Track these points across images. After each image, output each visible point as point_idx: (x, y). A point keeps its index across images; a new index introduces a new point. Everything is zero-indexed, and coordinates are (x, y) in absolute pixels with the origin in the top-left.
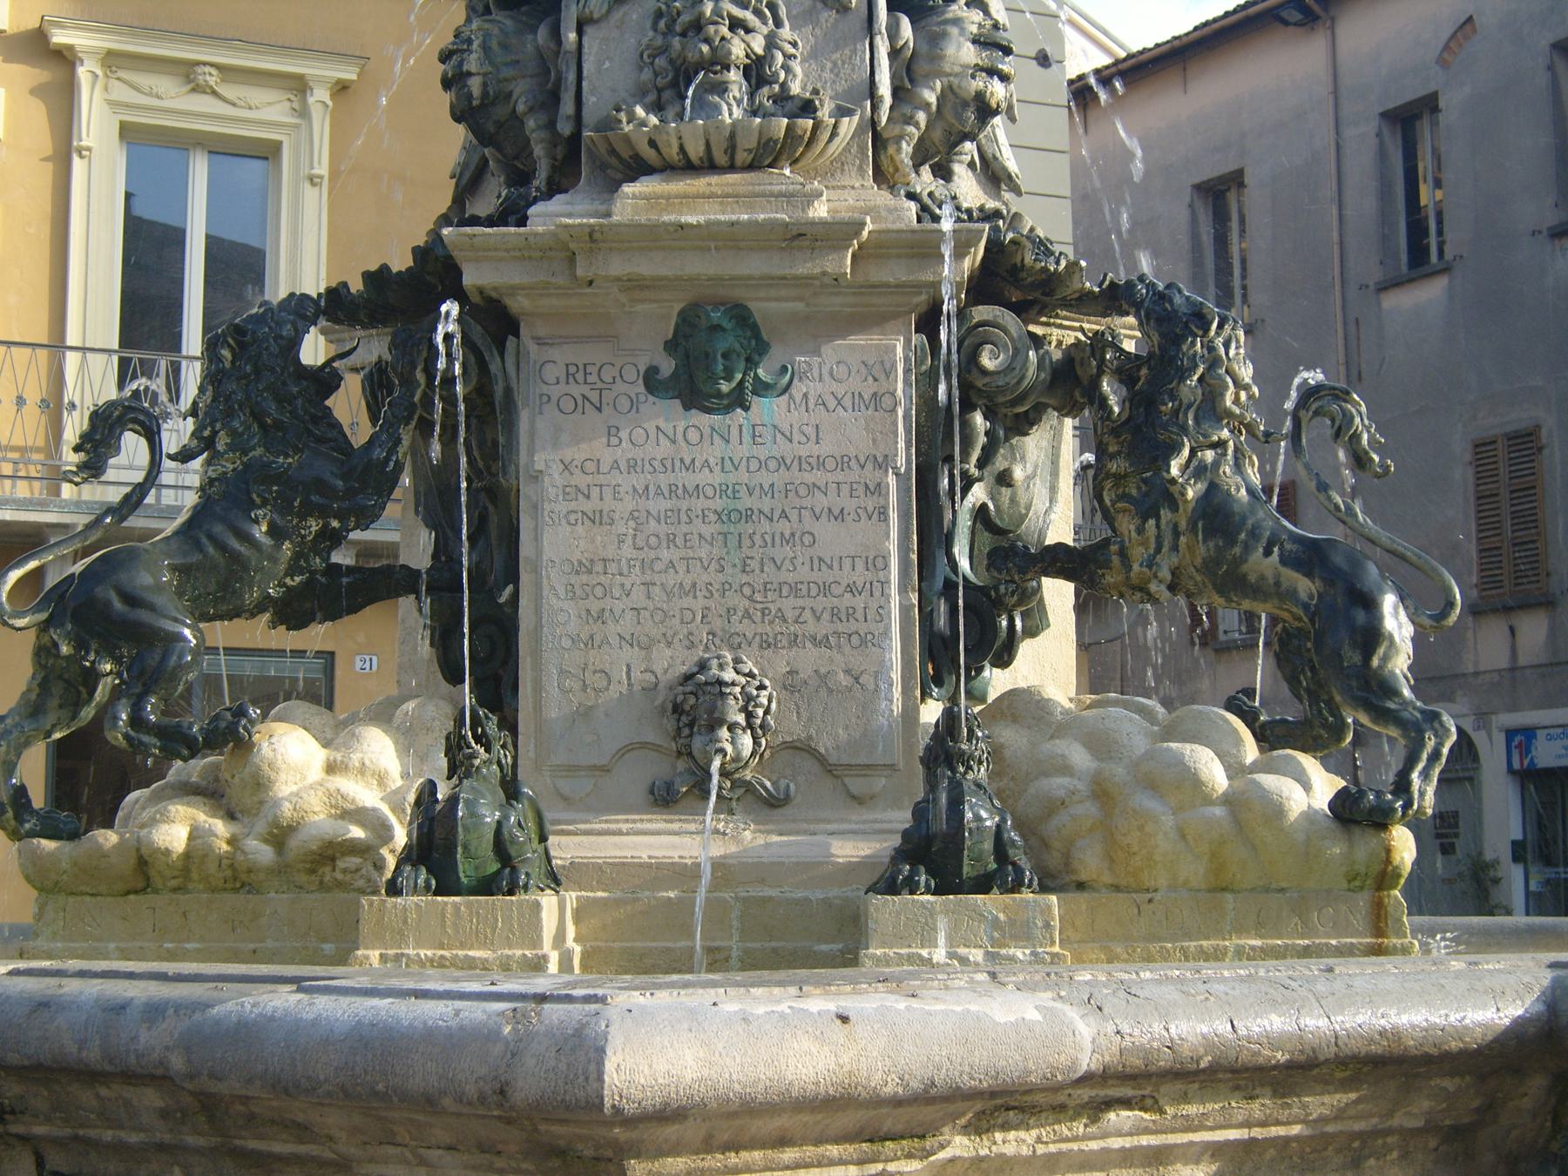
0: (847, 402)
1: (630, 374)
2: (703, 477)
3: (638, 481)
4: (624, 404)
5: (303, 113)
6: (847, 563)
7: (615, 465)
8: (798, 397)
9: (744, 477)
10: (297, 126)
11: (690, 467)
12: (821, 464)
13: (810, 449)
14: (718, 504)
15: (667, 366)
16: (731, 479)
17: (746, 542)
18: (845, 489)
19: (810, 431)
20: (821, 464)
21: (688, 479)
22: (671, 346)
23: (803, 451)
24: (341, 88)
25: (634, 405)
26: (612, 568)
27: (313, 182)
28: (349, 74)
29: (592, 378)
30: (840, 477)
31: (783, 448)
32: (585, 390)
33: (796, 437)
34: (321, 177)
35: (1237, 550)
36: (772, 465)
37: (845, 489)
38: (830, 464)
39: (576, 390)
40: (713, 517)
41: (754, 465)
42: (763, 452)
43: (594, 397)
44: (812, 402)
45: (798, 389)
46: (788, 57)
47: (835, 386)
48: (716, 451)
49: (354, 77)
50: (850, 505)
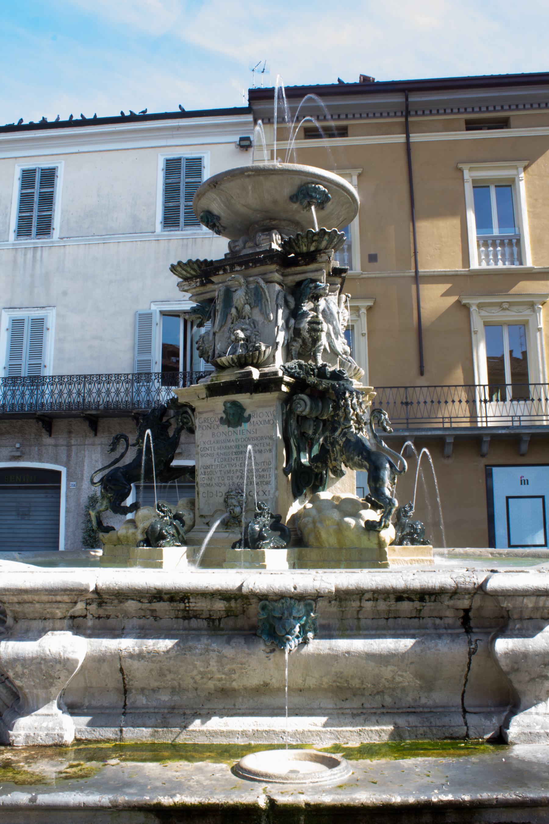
0: (262, 423)
1: (217, 420)
2: (232, 444)
3: (219, 445)
4: (216, 426)
5: (359, 316)
6: (262, 464)
7: (214, 442)
8: (252, 422)
9: (240, 443)
10: (357, 320)
11: (229, 441)
12: (257, 439)
13: (257, 435)
14: (235, 450)
15: (224, 416)
16: (237, 444)
17: (241, 459)
18: (262, 445)
19: (254, 431)
20: (257, 439)
21: (229, 444)
22: (224, 412)
23: (253, 436)
24: (369, 309)
25: (218, 427)
26: (214, 467)
27: (363, 335)
28: (371, 303)
29: (209, 421)
30: (261, 442)
31: (249, 435)
32: (208, 424)
33: (252, 432)
34: (365, 334)
35: (352, 456)
36: (247, 439)
37: (262, 445)
38: (259, 439)
39: (206, 424)
40: (234, 454)
41: (243, 440)
42: (244, 437)
43: (209, 425)
44: (255, 423)
45: (252, 420)
46: (256, 335)
47: (259, 419)
48: (234, 437)
49: (372, 304)
50: (263, 449)
